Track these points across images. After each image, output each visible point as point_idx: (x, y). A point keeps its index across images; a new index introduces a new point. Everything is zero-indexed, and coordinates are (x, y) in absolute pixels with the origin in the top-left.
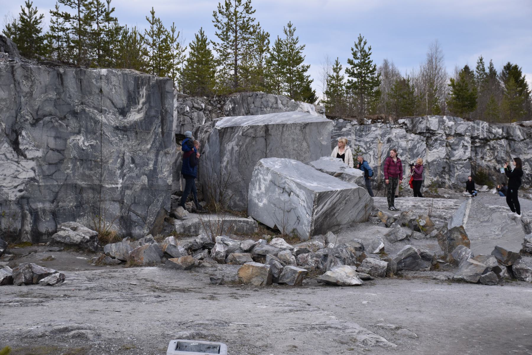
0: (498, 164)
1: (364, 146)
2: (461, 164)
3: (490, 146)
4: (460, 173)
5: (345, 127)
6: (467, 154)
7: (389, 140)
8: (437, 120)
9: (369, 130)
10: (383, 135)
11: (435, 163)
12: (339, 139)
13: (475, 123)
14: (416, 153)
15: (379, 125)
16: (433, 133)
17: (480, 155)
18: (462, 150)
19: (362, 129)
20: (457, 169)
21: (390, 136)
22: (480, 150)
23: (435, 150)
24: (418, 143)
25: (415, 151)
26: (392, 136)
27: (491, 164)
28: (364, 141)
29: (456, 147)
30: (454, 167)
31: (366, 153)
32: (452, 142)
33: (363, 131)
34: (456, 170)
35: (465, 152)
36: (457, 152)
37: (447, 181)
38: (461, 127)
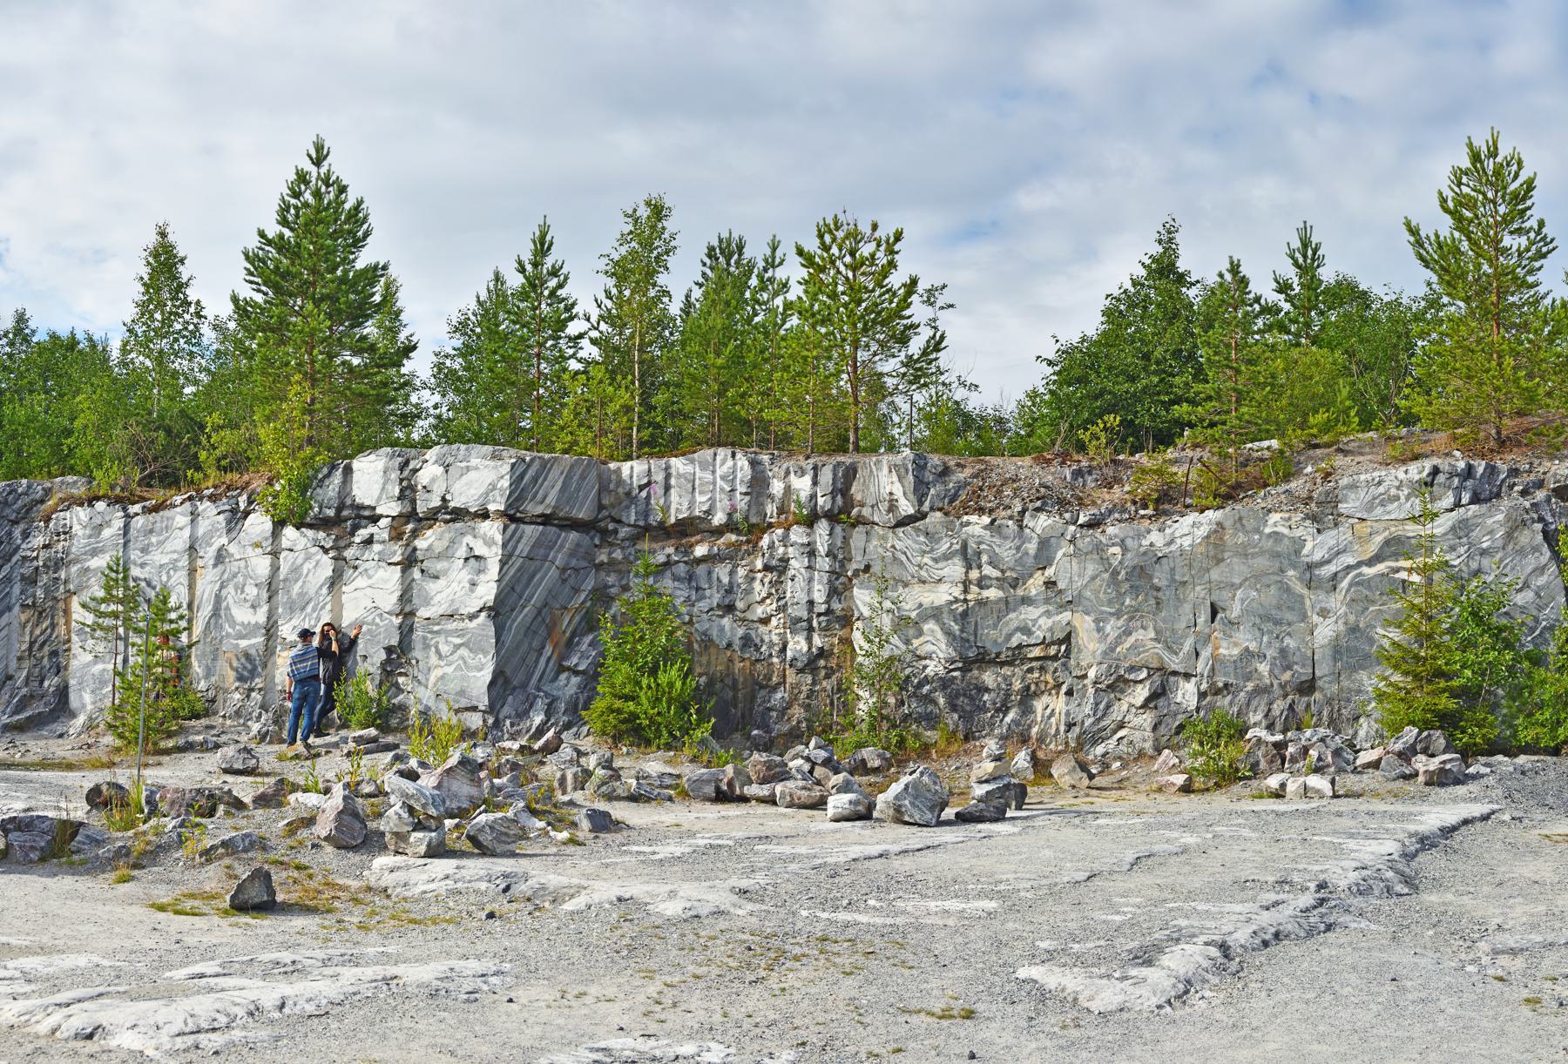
2: (460, 633)
4: (449, 670)
6: (480, 590)
13: (692, 461)
14: (302, 595)
20: (438, 652)
23: (361, 582)
29: (440, 566)
34: (434, 659)
36: (442, 582)
38: (469, 484)
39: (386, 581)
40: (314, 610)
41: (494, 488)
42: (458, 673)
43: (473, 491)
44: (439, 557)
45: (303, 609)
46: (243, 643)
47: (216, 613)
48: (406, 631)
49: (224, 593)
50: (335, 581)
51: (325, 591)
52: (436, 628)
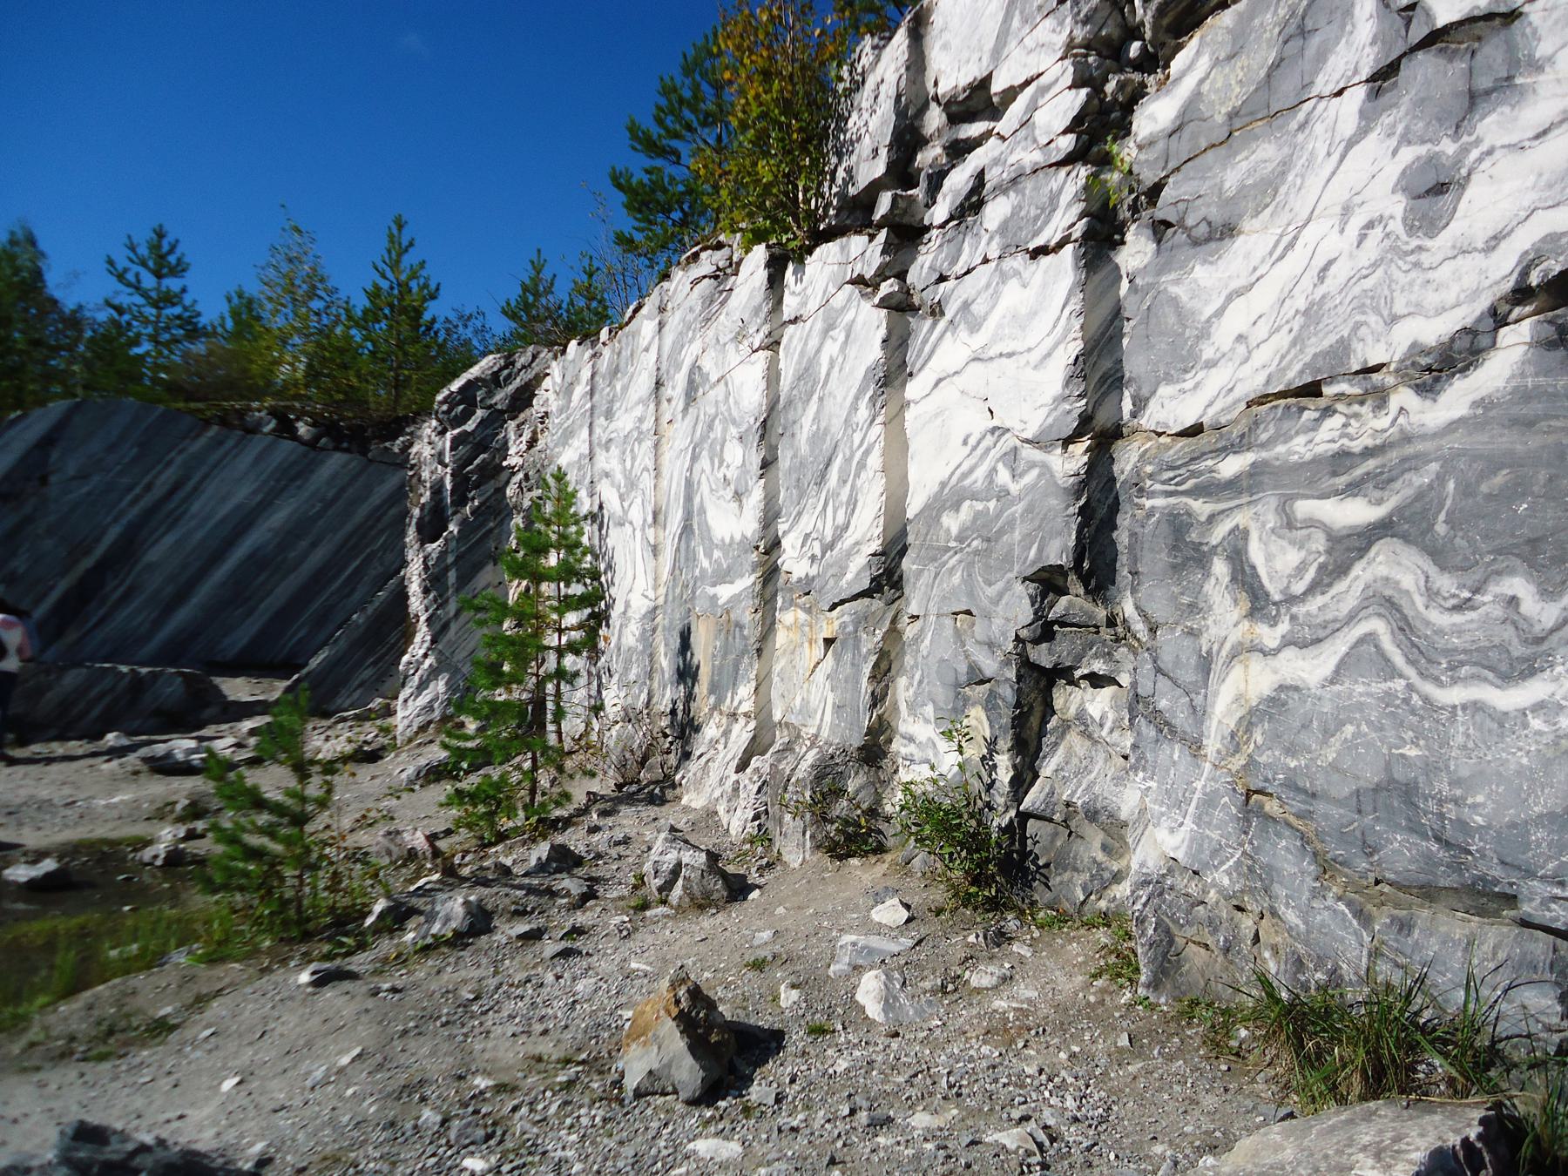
4: (1310, 669)
6: (1482, 205)
20: (1245, 580)
34: (1225, 617)
39: (1021, 322)
42: (1362, 689)
47: (687, 529)
48: (1098, 502)
50: (893, 373)
52: (1231, 466)
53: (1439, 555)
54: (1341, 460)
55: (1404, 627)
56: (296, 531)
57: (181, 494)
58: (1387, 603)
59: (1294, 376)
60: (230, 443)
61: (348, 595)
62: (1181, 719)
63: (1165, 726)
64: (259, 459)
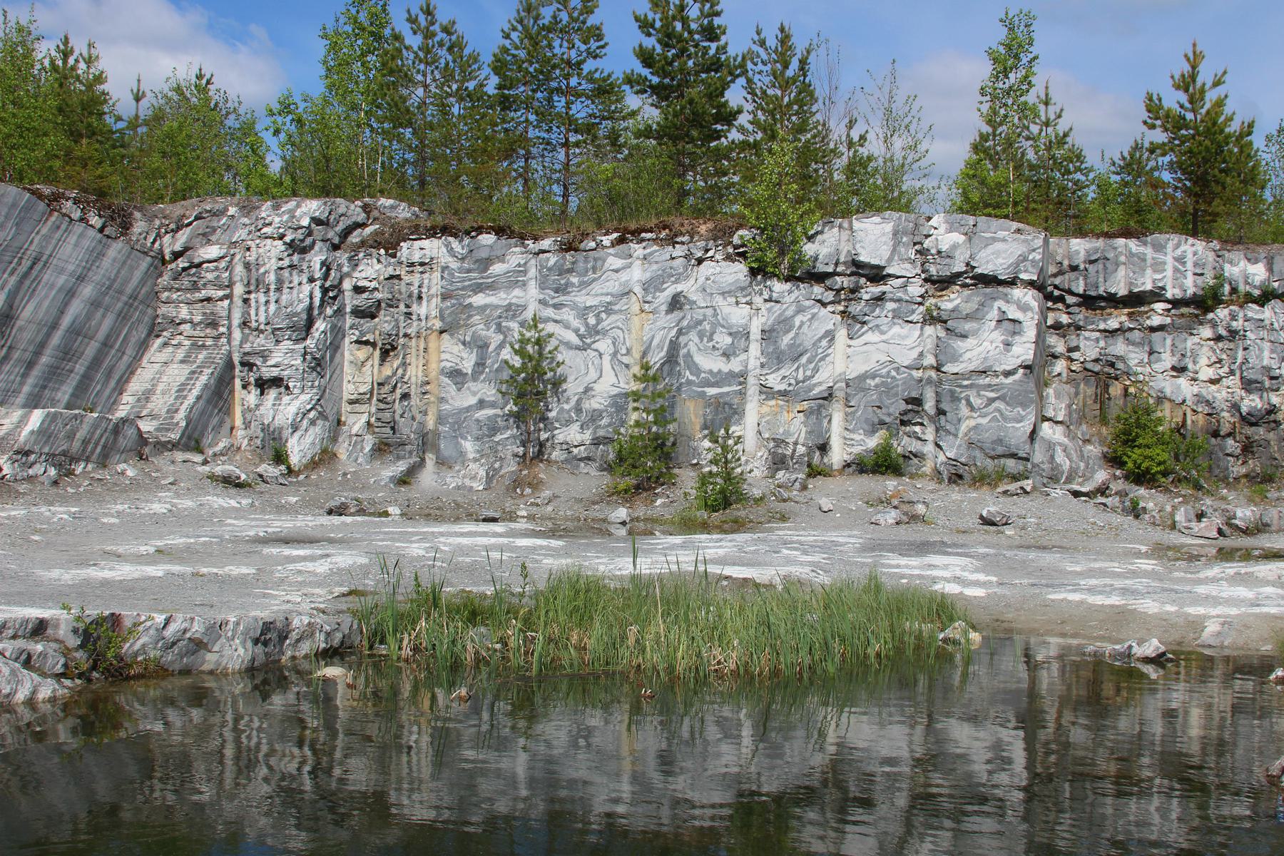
0: (1249, 391)
1: (576, 323)
3: (1214, 325)
4: (984, 421)
5: (502, 259)
6: (1016, 350)
7: (676, 303)
8: (889, 227)
9: (594, 269)
10: (651, 286)
11: (872, 383)
12: (479, 300)
13: (1145, 244)
14: (791, 346)
15: (638, 250)
16: (877, 275)
17: (1168, 360)
18: (999, 336)
19: (568, 265)
20: (969, 404)
21: (679, 287)
22: (1169, 342)
24: (800, 310)
25: (786, 340)
26: (687, 287)
27: (1219, 395)
28: (574, 307)
29: (968, 326)
30: (955, 399)
31: (584, 348)
32: (949, 306)
33: (570, 271)
34: (964, 411)
35: (1008, 345)
36: (970, 342)
37: (929, 448)
38: (997, 254)
39: (904, 338)
40: (810, 361)
41: (1025, 259)
43: (1001, 261)
44: (968, 317)
45: (797, 359)
46: (712, 391)
49: (683, 340)
51: (824, 343)
52: (966, 383)
53: (1008, 404)
54: (990, 386)
55: (1002, 414)
56: (95, 304)
57: (38, 267)
58: (999, 411)
59: (980, 369)
60: (64, 227)
61: (121, 358)
62: (953, 430)
63: (948, 432)
64: (76, 245)
